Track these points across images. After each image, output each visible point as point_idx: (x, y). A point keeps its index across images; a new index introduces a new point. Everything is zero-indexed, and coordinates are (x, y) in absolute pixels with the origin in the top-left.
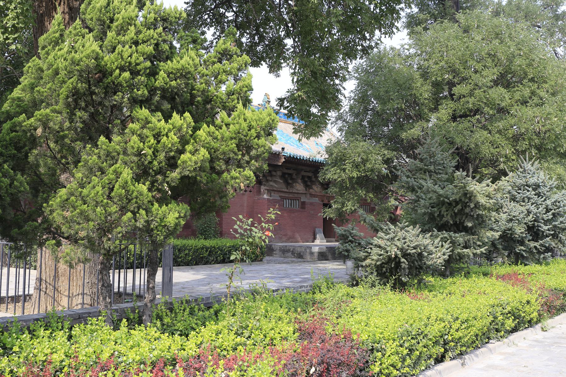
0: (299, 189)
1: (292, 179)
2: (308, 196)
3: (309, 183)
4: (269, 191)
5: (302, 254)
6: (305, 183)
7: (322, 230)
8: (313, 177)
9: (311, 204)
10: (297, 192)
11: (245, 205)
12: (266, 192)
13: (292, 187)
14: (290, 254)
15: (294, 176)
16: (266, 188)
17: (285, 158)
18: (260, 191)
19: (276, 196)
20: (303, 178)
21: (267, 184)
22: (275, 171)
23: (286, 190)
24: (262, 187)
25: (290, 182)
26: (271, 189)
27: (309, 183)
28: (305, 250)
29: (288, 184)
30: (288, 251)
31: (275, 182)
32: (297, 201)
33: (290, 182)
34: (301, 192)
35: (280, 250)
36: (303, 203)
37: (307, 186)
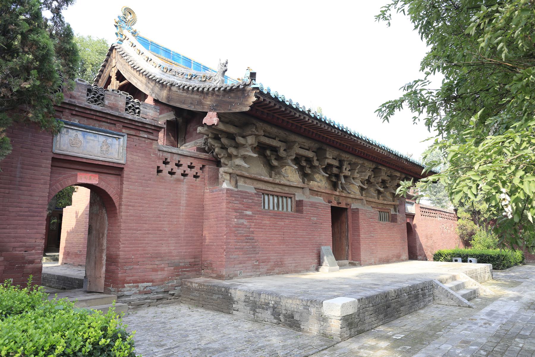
0: (293, 179)
1: (279, 158)
2: (308, 192)
3: (308, 171)
4: (235, 177)
5: (297, 317)
6: (301, 169)
7: (330, 248)
8: (315, 158)
9: (313, 205)
11: (183, 202)
12: (228, 177)
13: (279, 173)
14: (267, 315)
15: (282, 153)
16: (226, 169)
17: (256, 97)
18: (218, 178)
19: (249, 188)
20: (297, 160)
21: (230, 163)
22: (244, 137)
23: (267, 178)
24: (221, 170)
25: (275, 163)
26: (238, 172)
27: (308, 171)
28: (306, 307)
29: (271, 168)
30: (265, 306)
31: (245, 158)
32: (289, 200)
33: (275, 163)
34: (295, 184)
35: (247, 301)
36: (299, 204)
37: (305, 176)
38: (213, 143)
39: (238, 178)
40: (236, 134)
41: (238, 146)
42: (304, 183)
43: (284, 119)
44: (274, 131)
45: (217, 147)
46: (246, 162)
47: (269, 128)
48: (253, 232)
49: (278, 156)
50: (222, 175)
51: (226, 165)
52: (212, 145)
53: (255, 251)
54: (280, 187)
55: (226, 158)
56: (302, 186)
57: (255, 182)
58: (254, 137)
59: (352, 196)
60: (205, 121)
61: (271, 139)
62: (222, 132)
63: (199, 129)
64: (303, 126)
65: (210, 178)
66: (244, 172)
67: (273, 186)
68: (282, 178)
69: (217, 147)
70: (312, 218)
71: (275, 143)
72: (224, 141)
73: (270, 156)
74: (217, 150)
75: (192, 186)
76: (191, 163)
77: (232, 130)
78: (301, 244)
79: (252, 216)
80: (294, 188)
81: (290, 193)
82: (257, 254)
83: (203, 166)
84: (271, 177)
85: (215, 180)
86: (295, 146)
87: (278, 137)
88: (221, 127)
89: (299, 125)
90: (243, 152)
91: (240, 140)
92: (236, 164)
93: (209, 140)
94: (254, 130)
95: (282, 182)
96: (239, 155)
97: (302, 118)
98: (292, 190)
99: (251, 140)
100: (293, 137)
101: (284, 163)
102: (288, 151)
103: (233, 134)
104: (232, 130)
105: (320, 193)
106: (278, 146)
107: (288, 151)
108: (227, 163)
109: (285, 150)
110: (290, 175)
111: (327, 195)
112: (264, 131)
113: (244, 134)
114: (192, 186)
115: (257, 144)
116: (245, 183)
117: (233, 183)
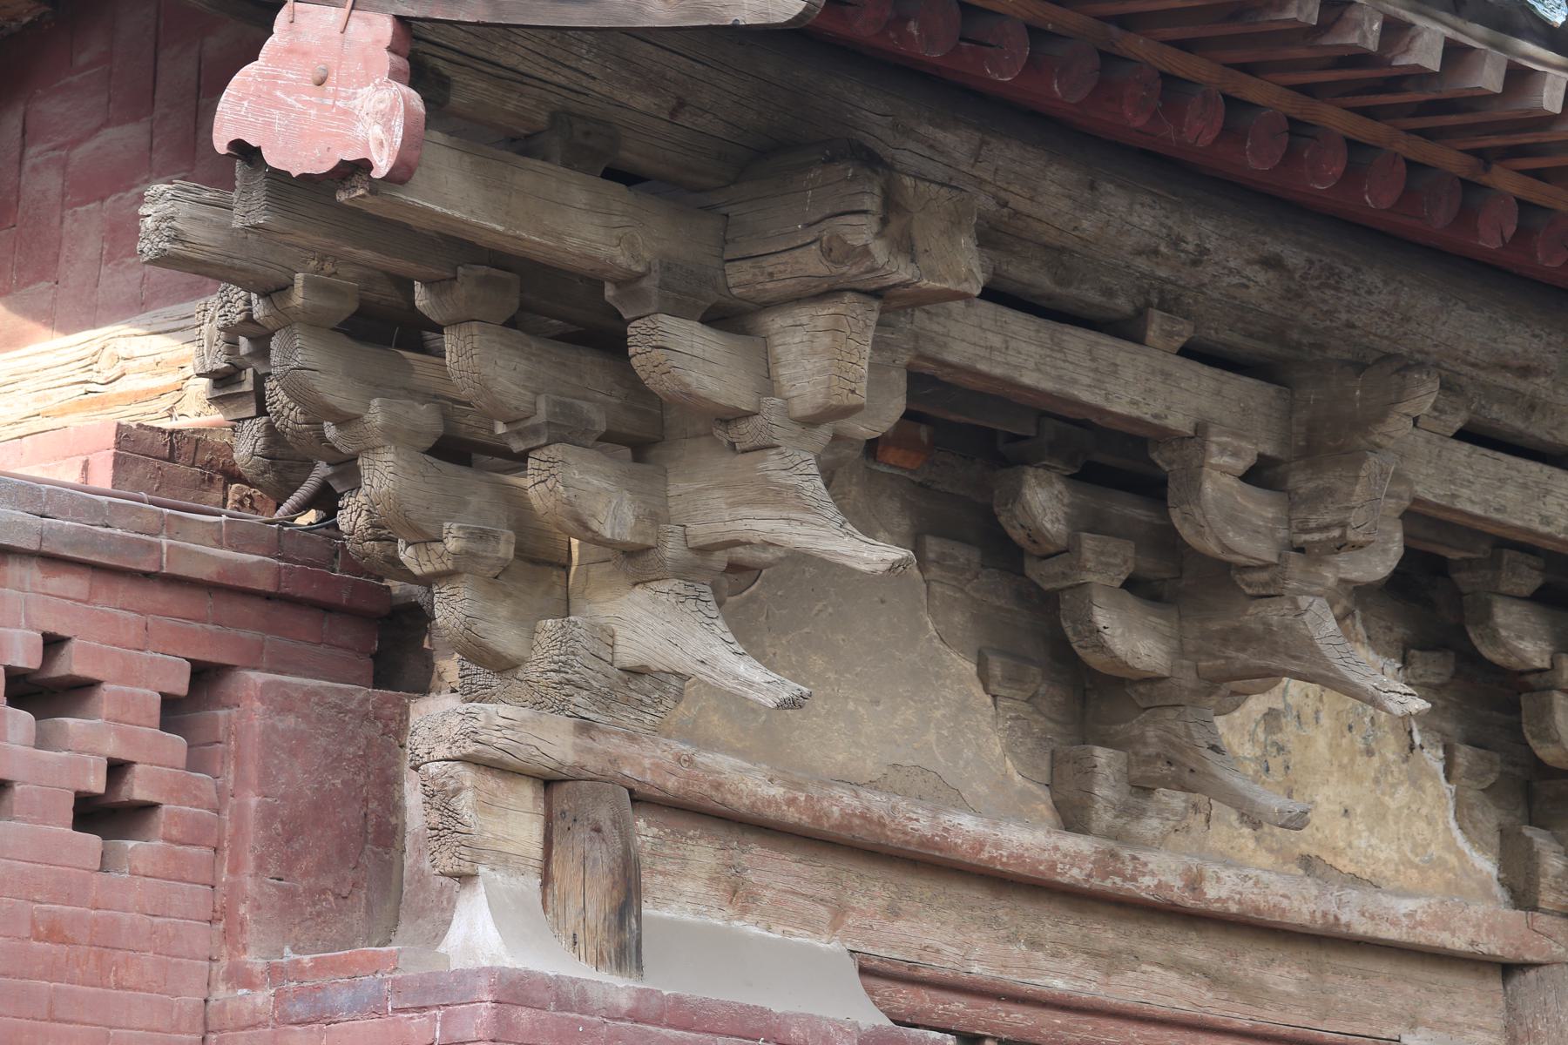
0: (1368, 846)
1: (1177, 578)
4: (607, 824)
10: (1302, 903)
12: (517, 823)
13: (1183, 772)
15: (1228, 513)
16: (503, 721)
18: (384, 833)
20: (1432, 597)
21: (543, 645)
22: (729, 318)
23: (1028, 840)
24: (438, 719)
25: (1131, 639)
26: (651, 759)
29: (1080, 700)
31: (737, 581)
33: (1131, 639)
34: (1401, 915)
38: (334, 390)
39: (645, 831)
40: (628, 282)
41: (647, 433)
42: (1522, 895)
43: (1252, 90)
44: (1127, 224)
45: (391, 434)
46: (747, 637)
47: (1051, 194)
49: (1167, 543)
50: (441, 797)
51: (503, 666)
52: (318, 412)
54: (1198, 949)
55: (498, 580)
56: (1491, 946)
57: (870, 891)
58: (860, 317)
60: (238, 113)
61: (1077, 339)
62: (456, 250)
63: (162, 206)
64: (1506, 180)
65: (289, 832)
66: (723, 763)
67: (1107, 934)
68: (1228, 832)
69: (391, 434)
71: (1130, 384)
72: (478, 362)
73: (1069, 550)
74: (383, 477)
75: (54, 933)
76: (53, 643)
77: (582, 227)
80: (1383, 968)
83: (205, 676)
84: (1072, 817)
85: (356, 856)
86: (1397, 427)
87: (1170, 304)
88: (455, 196)
89: (1450, 159)
90: (716, 506)
91: (687, 356)
92: (628, 654)
93: (294, 354)
94: (861, 232)
95: (1222, 891)
96: (672, 549)
97: (1489, 77)
99: (821, 361)
100: (1381, 303)
101: (1245, 638)
102: (1302, 482)
103: (595, 284)
104: (582, 227)
106: (1179, 421)
107: (1302, 482)
108: (505, 638)
109: (1259, 475)
110: (1326, 796)
112: (990, 237)
113: (740, 279)
114: (54, 933)
115: (895, 407)
116: (739, 894)
117: (590, 899)
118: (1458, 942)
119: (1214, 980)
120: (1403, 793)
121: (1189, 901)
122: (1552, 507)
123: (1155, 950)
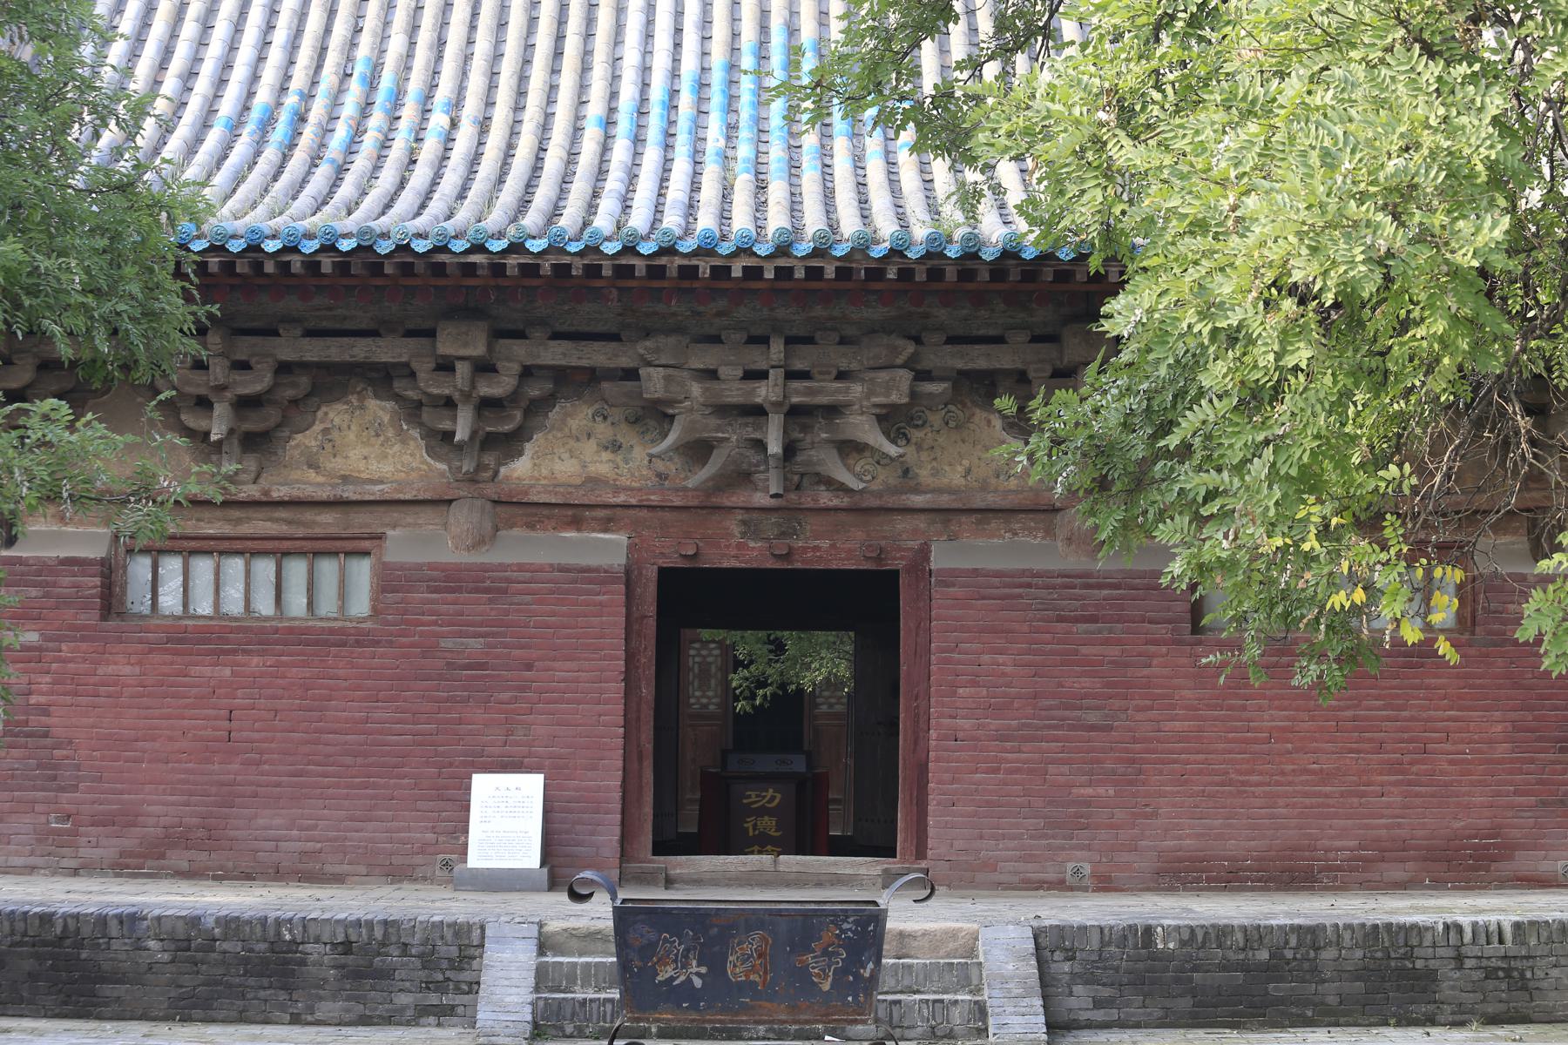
48: (44, 710)
53: (55, 778)
59: (918, 500)
70: (447, 643)
78: (349, 760)
79: (39, 649)
80: (382, 509)
81: (345, 533)
82: (62, 789)
98: (362, 521)
105: (601, 513)
111: (667, 515)
118: (408, 497)
119: (289, 522)
120: (397, 448)
121: (264, 499)
122: (356, 351)
123: (260, 516)
